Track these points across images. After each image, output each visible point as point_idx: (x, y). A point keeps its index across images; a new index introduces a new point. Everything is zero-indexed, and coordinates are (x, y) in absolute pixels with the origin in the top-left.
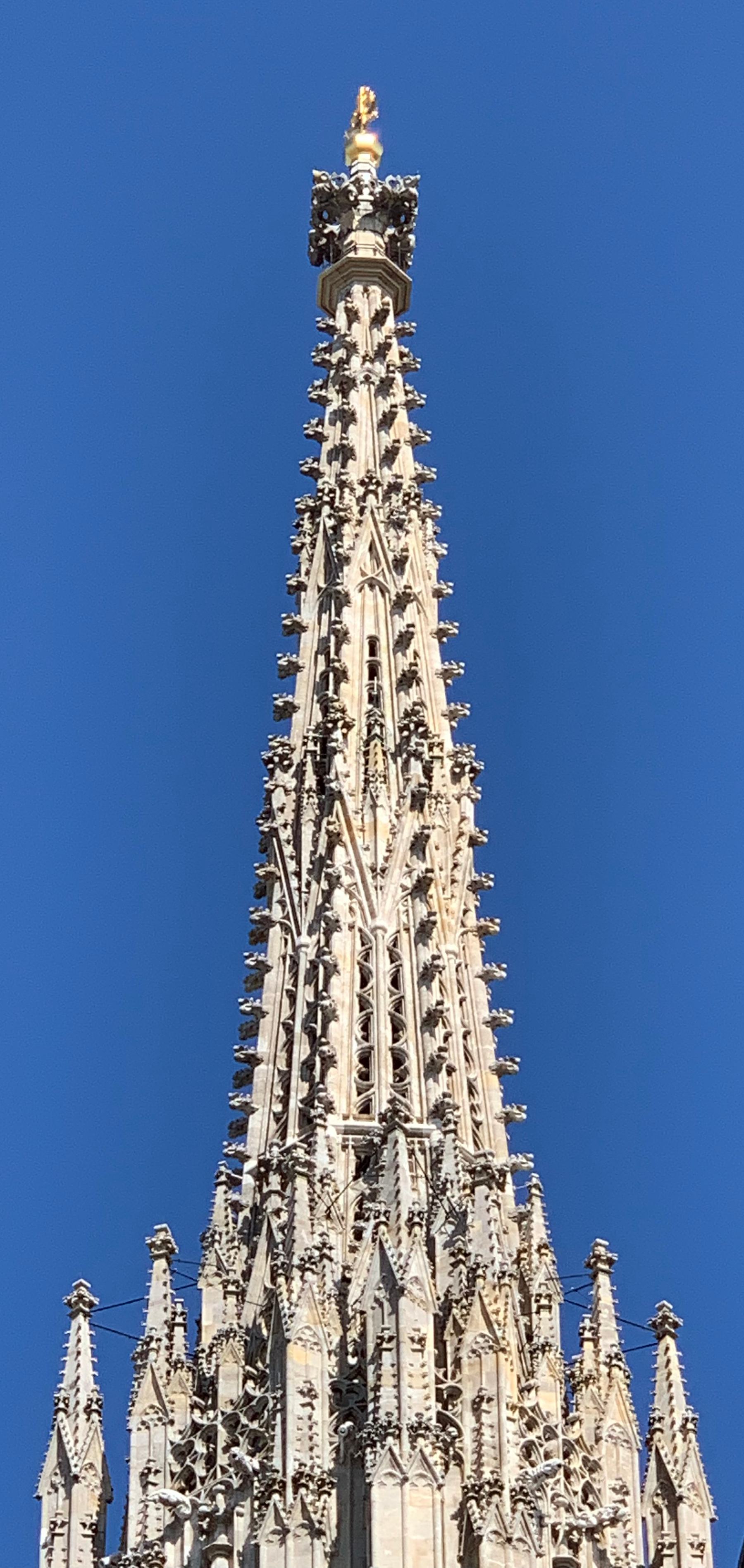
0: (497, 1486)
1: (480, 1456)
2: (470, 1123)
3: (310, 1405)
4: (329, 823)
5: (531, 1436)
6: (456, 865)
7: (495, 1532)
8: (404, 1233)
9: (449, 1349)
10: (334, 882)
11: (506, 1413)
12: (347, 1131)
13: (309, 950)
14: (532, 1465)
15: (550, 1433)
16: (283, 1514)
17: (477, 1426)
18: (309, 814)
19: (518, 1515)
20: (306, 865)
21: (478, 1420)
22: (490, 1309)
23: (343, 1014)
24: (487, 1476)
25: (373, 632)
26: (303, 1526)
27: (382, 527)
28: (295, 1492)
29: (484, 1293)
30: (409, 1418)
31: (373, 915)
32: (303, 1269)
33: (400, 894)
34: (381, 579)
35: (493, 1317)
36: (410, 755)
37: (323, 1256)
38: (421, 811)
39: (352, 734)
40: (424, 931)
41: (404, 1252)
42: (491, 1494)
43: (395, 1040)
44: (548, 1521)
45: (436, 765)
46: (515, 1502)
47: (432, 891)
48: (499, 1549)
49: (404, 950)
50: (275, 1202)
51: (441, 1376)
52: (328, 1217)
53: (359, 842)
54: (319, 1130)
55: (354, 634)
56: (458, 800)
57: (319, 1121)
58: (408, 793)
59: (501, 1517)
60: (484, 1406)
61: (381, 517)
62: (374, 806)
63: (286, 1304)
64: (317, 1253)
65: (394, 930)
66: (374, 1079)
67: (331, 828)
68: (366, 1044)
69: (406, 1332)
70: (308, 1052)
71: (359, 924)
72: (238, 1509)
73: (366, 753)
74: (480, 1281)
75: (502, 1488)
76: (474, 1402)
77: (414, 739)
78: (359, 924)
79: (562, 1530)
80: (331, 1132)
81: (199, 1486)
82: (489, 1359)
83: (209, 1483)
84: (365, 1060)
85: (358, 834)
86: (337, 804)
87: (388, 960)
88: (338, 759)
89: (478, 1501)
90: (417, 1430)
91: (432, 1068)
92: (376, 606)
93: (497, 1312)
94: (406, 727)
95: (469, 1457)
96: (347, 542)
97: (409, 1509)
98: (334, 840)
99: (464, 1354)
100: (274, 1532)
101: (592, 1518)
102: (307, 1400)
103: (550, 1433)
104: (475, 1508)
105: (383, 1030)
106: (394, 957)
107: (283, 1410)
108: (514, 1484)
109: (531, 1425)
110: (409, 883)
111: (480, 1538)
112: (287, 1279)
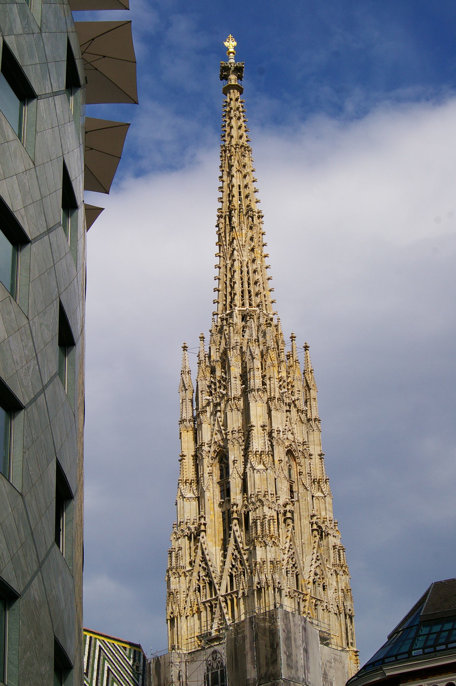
0: (275, 397)
1: (271, 391)
2: (265, 305)
3: (236, 380)
4: (232, 235)
5: (281, 383)
6: (259, 241)
7: (274, 408)
8: (254, 343)
9: (263, 365)
10: (234, 249)
11: (276, 380)
12: (239, 311)
13: (229, 264)
14: (281, 390)
15: (284, 381)
16: (232, 406)
17: (270, 383)
18: (228, 231)
19: (279, 404)
20: (228, 242)
21: (270, 382)
22: (272, 357)
23: (237, 282)
25: (239, 184)
26: (236, 408)
27: (240, 156)
28: (234, 401)
29: (270, 353)
31: (243, 257)
32: (232, 348)
33: (248, 251)
34: (240, 170)
35: (272, 359)
36: (249, 216)
37: (237, 345)
38: (252, 230)
39: (236, 211)
40: (254, 261)
41: (254, 348)
42: (273, 400)
43: (249, 287)
44: (285, 402)
45: (254, 217)
46: (278, 401)
47: (255, 250)
48: (275, 412)
49: (249, 265)
52: (237, 333)
53: (239, 239)
54: (234, 312)
55: (235, 185)
56: (259, 224)
57: (234, 310)
58: (249, 226)
59: (275, 405)
60: (271, 379)
61: (240, 154)
62: (242, 230)
63: (230, 357)
65: (247, 260)
66: (245, 298)
67: (233, 236)
68: (243, 289)
69: (255, 367)
70: (230, 290)
71: (240, 259)
72: (222, 402)
73: (239, 215)
74: (269, 350)
75: (275, 398)
76: (269, 378)
77: (250, 212)
78: (240, 259)
79: (287, 403)
80: (236, 311)
81: (213, 395)
82: (272, 368)
83: (215, 395)
84: (242, 292)
85: (238, 237)
86: (234, 229)
87: (246, 268)
88: (233, 218)
89: (271, 401)
90: (258, 390)
91: (257, 295)
92: (240, 176)
93: (273, 357)
94: (248, 209)
95: (268, 390)
96: (233, 161)
97: (258, 407)
98: (233, 239)
99: (266, 367)
100: (230, 409)
101: (293, 398)
102: (235, 379)
103: (284, 381)
104: (270, 403)
105: (246, 285)
106: (247, 267)
107: (230, 381)
109: (280, 381)
110: (250, 248)
111: (271, 410)
112: (230, 351)
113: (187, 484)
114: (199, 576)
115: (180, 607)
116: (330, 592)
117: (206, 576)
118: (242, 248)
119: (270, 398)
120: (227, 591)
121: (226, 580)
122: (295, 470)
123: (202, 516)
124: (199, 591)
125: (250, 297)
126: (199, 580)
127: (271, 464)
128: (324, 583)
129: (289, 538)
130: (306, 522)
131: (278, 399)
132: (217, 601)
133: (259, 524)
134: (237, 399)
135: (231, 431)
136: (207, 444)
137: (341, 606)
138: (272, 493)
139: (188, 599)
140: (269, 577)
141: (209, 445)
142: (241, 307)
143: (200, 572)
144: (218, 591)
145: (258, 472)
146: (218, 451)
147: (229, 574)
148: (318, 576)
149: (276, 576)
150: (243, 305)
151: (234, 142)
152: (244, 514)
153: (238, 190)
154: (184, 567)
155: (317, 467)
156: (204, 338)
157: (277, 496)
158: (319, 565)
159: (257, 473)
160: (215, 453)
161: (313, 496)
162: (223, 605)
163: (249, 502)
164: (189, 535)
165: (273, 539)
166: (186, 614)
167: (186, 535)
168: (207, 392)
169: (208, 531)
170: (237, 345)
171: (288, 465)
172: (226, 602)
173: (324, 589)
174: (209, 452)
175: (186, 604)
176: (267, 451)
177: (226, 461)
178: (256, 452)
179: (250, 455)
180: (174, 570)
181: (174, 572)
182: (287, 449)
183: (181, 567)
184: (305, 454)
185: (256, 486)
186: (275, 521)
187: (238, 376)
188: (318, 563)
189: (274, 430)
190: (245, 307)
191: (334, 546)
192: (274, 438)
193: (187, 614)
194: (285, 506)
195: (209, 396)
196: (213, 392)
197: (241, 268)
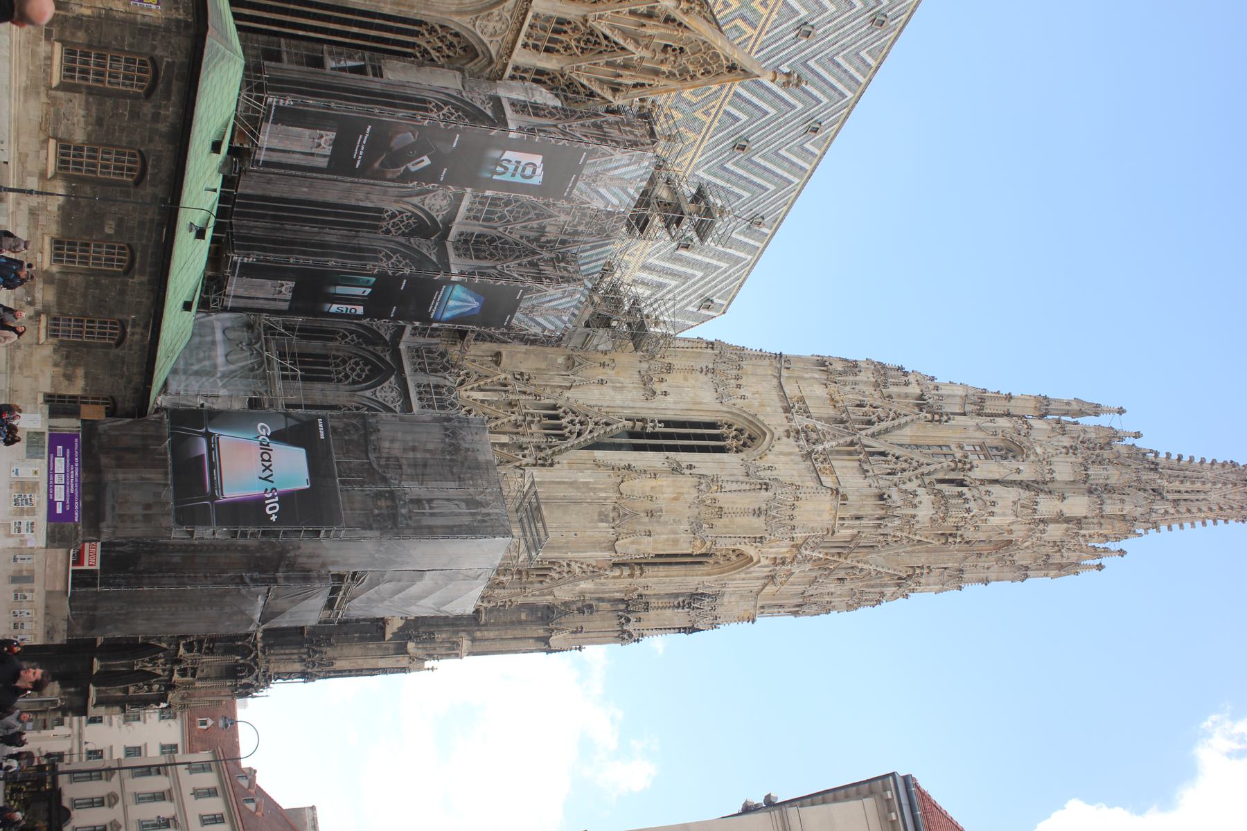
30: (1104, 507)
49: (1205, 502)
50: (1147, 466)
84: (1179, 492)
105: (1186, 496)
116: (832, 587)
117: (879, 417)
119: (1080, 523)
121: (878, 445)
122: (984, 548)
124: (858, 406)
130: (922, 560)
137: (813, 600)
139: (848, 388)
144: (863, 433)
148: (858, 573)
149: (897, 522)
152: (963, 480)
154: (885, 386)
161: (945, 568)
162: (849, 439)
165: (940, 521)
169: (930, 425)
172: (852, 444)
173: (839, 579)
187: (1108, 482)
188: (873, 573)
191: (883, 593)
196: (1085, 445)
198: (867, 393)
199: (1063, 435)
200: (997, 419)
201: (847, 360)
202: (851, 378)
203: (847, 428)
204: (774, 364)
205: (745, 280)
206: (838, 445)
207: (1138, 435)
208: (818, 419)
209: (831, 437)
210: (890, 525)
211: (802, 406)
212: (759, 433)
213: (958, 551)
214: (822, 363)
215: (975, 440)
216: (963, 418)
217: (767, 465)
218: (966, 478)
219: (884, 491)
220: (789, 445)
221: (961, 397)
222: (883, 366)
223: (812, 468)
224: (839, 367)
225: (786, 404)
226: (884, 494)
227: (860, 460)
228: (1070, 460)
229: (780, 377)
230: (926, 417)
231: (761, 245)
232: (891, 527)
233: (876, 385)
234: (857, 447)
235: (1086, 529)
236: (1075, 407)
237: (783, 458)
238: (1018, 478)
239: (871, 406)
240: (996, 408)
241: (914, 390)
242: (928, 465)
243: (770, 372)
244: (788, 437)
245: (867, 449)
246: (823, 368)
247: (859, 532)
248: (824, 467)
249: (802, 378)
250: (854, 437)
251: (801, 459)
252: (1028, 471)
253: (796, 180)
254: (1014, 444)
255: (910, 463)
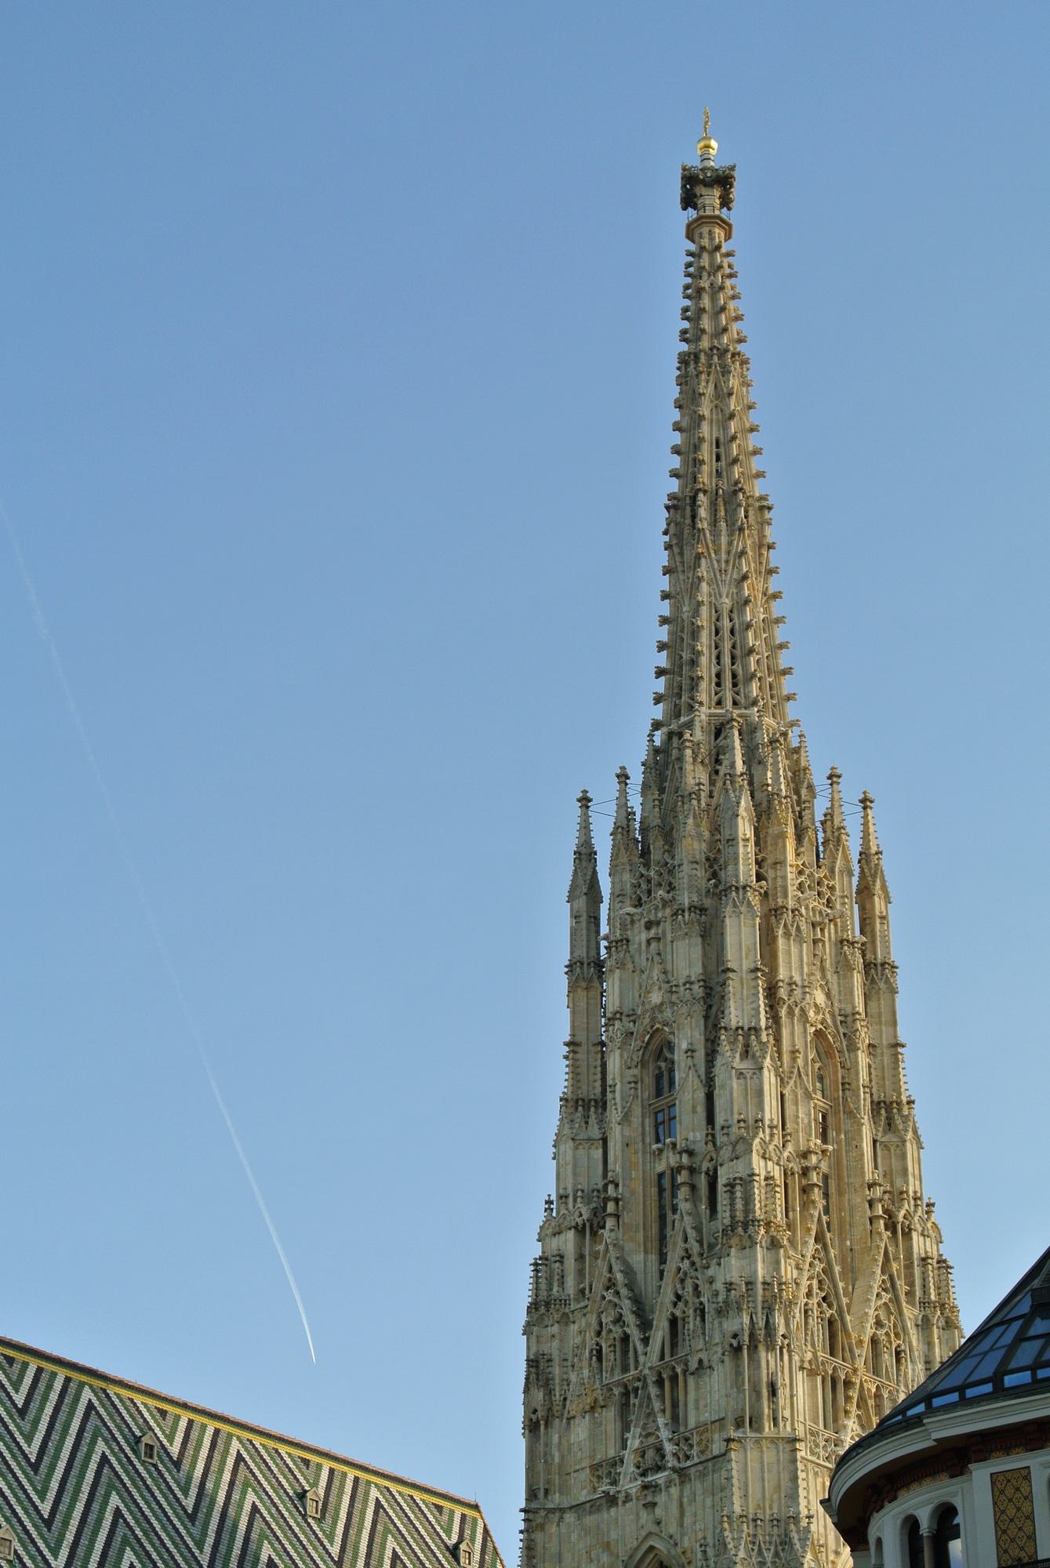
24: (780, 904)
31: (721, 597)
43: (733, 664)
51: (757, 851)
54: (696, 718)
64: (697, 788)
84: (718, 675)
87: (728, 621)
89: (776, 916)
108: (793, 907)
109: (801, 873)
111: (777, 936)
113: (580, 1108)
114: (601, 1324)
115: (555, 1395)
118: (718, 577)
120: (662, 1358)
121: (660, 1333)
123: (612, 1182)
125: (735, 685)
126: (599, 1334)
127: (771, 1059)
128: (899, 1346)
129: (813, 1233)
131: (793, 911)
132: (639, 1380)
133: (738, 1194)
134: (698, 912)
135: (681, 984)
136: (628, 1016)
138: (775, 1123)
139: (573, 1377)
140: (760, 1320)
141: (632, 1018)
142: (715, 708)
143: (602, 1312)
144: (642, 1359)
145: (742, 1076)
146: (651, 1032)
147: (670, 1317)
150: (719, 703)
151: (705, 343)
152: (707, 1173)
153: (715, 450)
154: (566, 1302)
155: (886, 1075)
156: (628, 778)
157: (784, 1133)
158: (887, 1301)
159: (738, 1078)
160: (644, 1036)
161: (875, 1142)
162: (653, 1390)
163: (718, 1144)
164: (579, 1228)
166: (569, 1412)
167: (574, 1227)
168: (631, 898)
169: (626, 1218)
170: (700, 790)
171: (817, 1065)
172: (660, 1382)
173: (898, 1361)
174: (632, 1033)
175: (569, 1390)
176: (763, 1027)
177: (669, 1055)
178: (737, 1029)
179: (723, 1037)
180: (543, 1309)
181: (544, 1314)
182: (813, 1029)
183: (561, 1300)
184: (857, 1041)
185: (736, 1110)
186: (777, 1189)
189: (783, 981)
190: (722, 708)
191: (924, 1260)
192: (781, 1003)
193: (571, 1413)
194: (805, 1155)
195: (636, 906)
196: (644, 899)
197: (718, 620)
198: (578, 1340)
199: (628, 941)
200: (609, 1082)
201: (527, 1378)
202: (556, 1370)
203: (636, 1390)
204: (540, 1521)
205: (414, 1486)
206: (664, 1411)
207: (623, 777)
208: (624, 1447)
209: (651, 1419)
210: (782, 1330)
211: (602, 1472)
212: (651, 1556)
213: (838, 1134)
214: (533, 1427)
215: (647, 1121)
216: (611, 1144)
217: (700, 1555)
218: (704, 1169)
219: (727, 1347)
220: (667, 1502)
221: (576, 1148)
222: (533, 1308)
223: (700, 1468)
224: (539, 1395)
225: (603, 1501)
226: (731, 1345)
227: (685, 1372)
228: (669, 937)
229: (560, 1509)
230: (612, 1230)
231: (352, 1473)
232: (787, 1325)
233: (565, 1320)
234: (665, 1376)
235: (786, 896)
236: (581, 903)
237: (688, 1521)
238: (701, 1054)
239: (599, 1334)
240: (592, 1070)
241: (568, 1242)
242: (686, 1240)
243: (554, 1529)
244: (654, 1505)
245: (667, 1358)
246: (542, 1427)
247: (802, 1368)
248: (699, 1444)
249: (560, 1466)
250: (649, 1381)
251: (688, 1486)
252: (688, 1036)
253: (235, 1445)
254: (648, 1043)
255: (685, 1274)
